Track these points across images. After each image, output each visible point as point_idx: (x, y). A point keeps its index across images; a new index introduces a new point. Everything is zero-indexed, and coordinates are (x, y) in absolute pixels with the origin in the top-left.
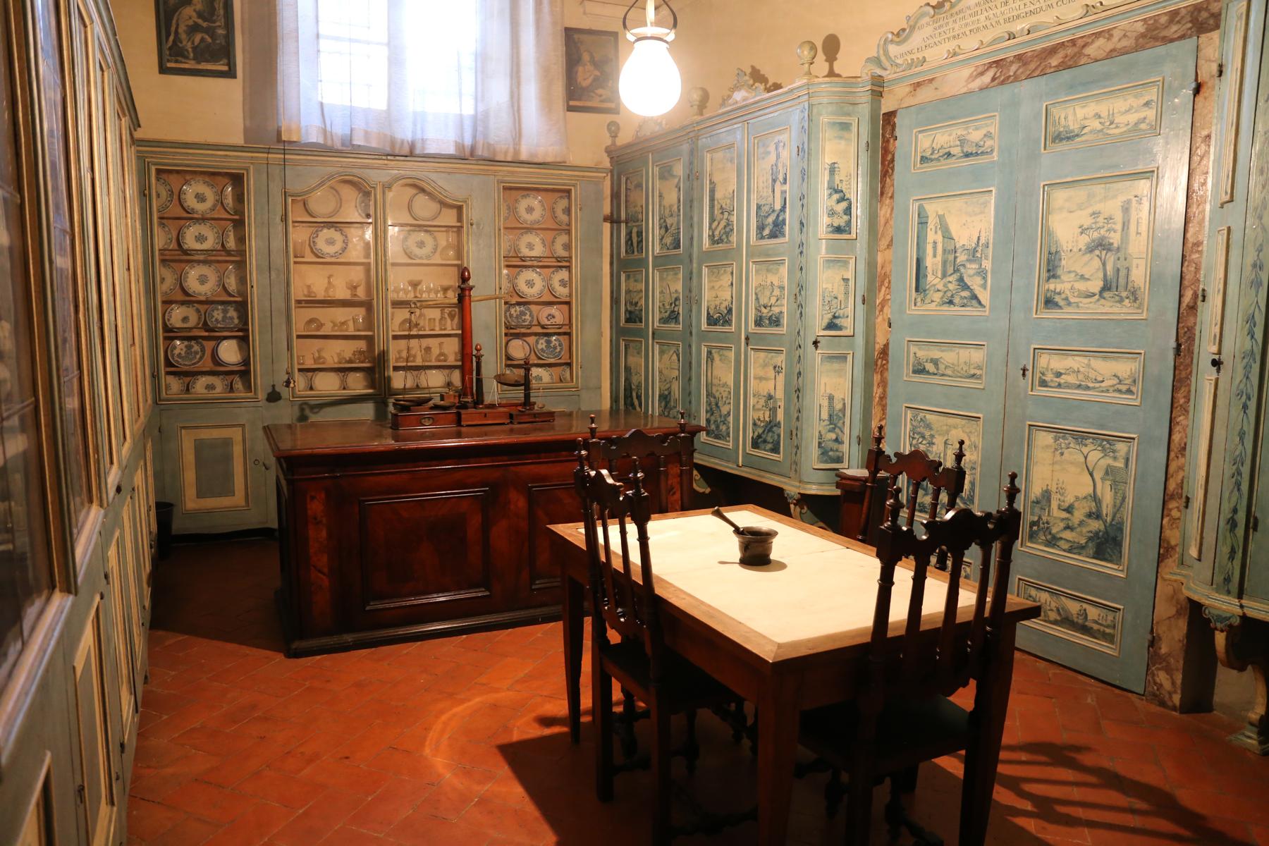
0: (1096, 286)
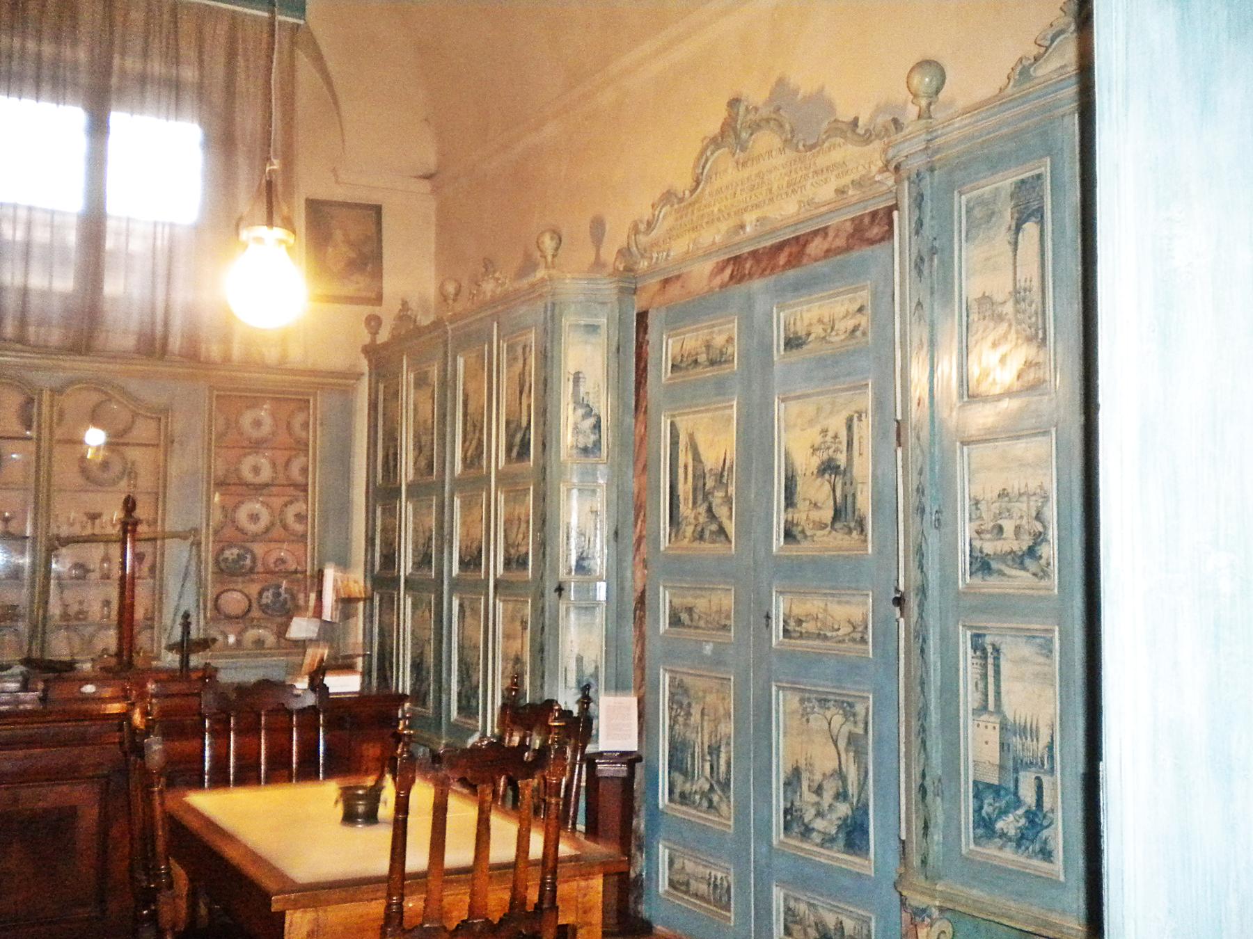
0: (828, 514)
